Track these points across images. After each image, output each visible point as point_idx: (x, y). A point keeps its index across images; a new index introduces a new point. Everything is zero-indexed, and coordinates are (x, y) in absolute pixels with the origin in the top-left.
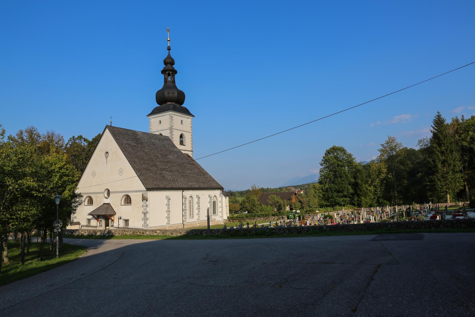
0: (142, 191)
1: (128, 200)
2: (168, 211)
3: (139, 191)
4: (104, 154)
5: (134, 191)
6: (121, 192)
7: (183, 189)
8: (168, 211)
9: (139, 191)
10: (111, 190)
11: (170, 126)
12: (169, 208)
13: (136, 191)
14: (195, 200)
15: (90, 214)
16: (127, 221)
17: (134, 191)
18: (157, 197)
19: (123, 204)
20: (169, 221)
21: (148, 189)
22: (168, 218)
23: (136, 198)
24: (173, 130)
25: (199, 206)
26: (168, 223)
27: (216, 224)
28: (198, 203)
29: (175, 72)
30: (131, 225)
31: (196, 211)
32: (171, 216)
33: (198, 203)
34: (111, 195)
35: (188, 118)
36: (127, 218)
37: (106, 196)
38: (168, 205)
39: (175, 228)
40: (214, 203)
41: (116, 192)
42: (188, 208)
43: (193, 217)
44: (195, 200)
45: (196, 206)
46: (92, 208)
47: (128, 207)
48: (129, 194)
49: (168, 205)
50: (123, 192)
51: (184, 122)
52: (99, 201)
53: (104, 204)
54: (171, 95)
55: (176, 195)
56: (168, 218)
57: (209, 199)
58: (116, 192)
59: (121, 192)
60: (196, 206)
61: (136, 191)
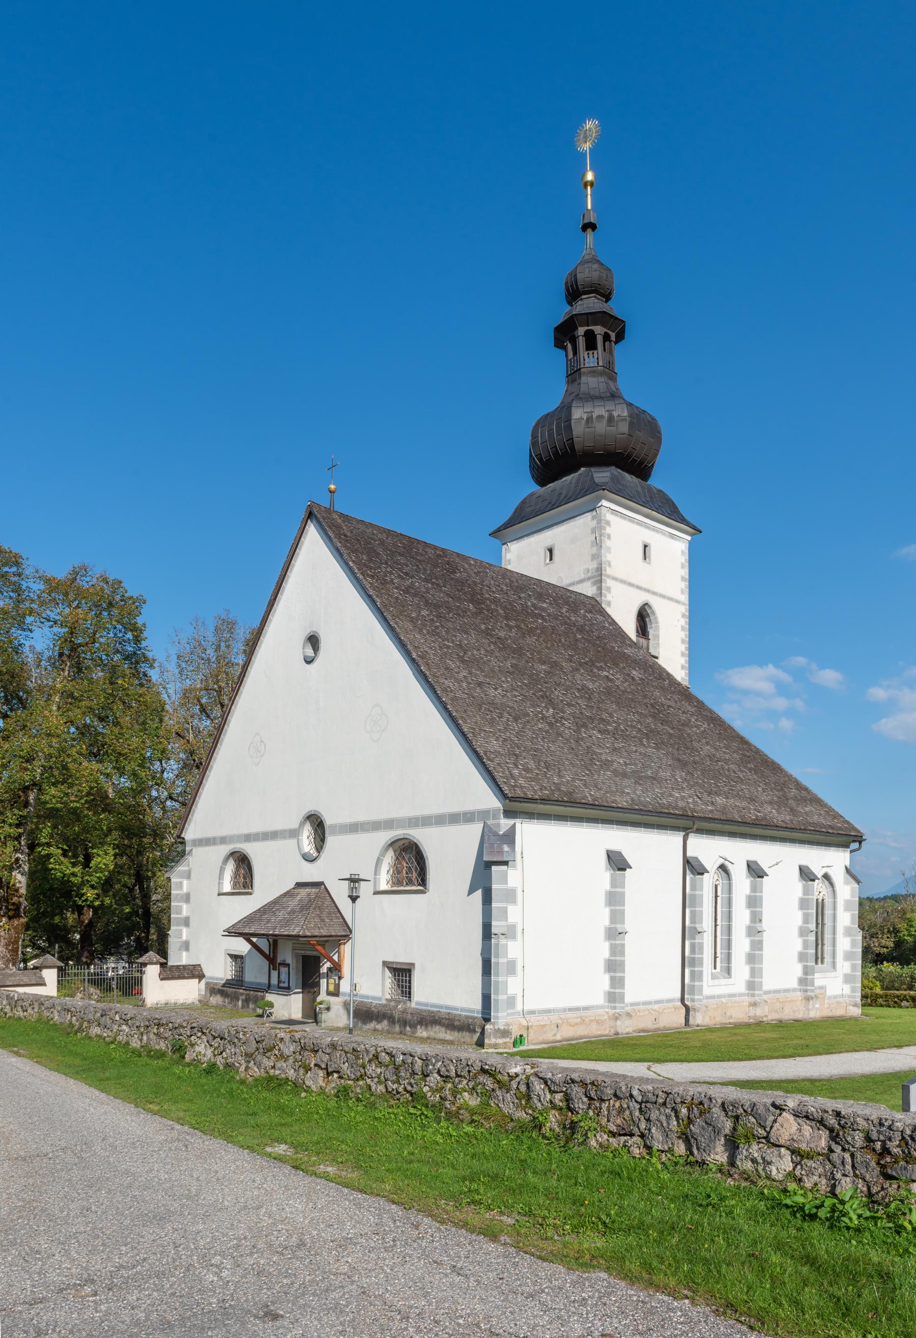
0: (483, 815)
1: (411, 865)
2: (615, 934)
3: (468, 817)
4: (299, 649)
5: (441, 820)
6: (377, 826)
7: (686, 822)
8: (615, 934)
9: (468, 817)
10: (328, 821)
11: (593, 565)
12: (617, 916)
13: (454, 819)
14: (742, 883)
15: (233, 932)
16: (402, 974)
17: (441, 820)
18: (556, 858)
19: (384, 886)
20: (617, 982)
21: (518, 805)
22: (614, 966)
23: (451, 855)
24: (609, 583)
25: (756, 918)
26: (614, 997)
27: (827, 1013)
28: (754, 902)
29: (618, 329)
30: (427, 993)
31: (741, 945)
32: (630, 959)
33: (754, 902)
34: (330, 840)
35: (672, 536)
36: (401, 958)
37: (308, 846)
38: (615, 899)
39: (648, 1024)
40: (820, 907)
41: (354, 828)
42: (707, 924)
43: (728, 971)
44: (742, 883)
45: (741, 917)
46: (242, 908)
47: (409, 905)
48: (419, 835)
49: (615, 899)
50: (389, 824)
51: (653, 552)
52: (279, 871)
53: (299, 885)
54: (601, 428)
55: (655, 853)
56: (614, 966)
57: (798, 886)
58: (354, 828)
59: (377, 826)
60: (741, 917)
61: (454, 819)
